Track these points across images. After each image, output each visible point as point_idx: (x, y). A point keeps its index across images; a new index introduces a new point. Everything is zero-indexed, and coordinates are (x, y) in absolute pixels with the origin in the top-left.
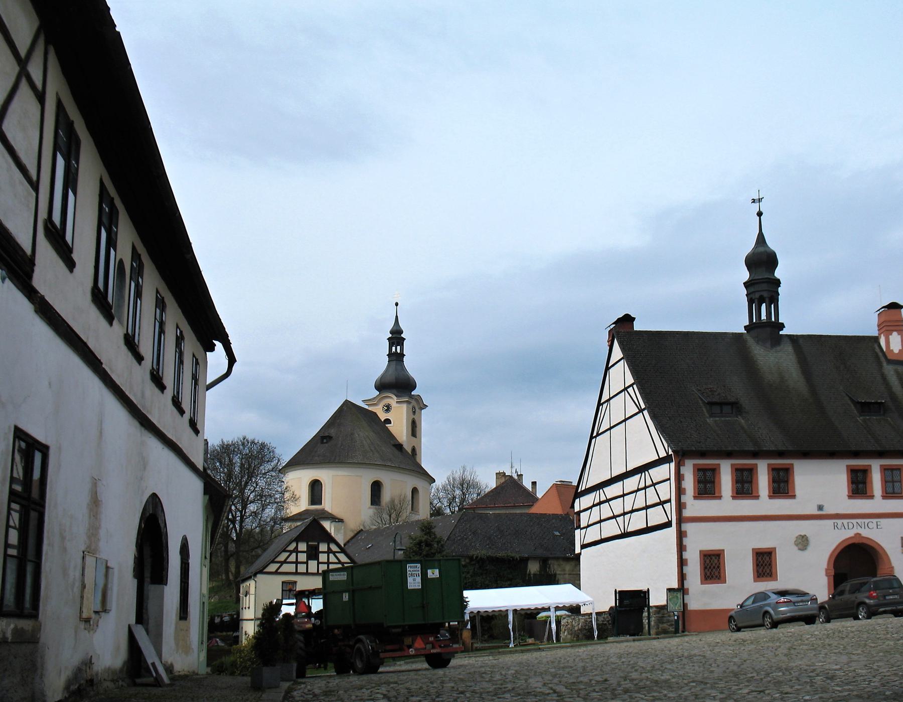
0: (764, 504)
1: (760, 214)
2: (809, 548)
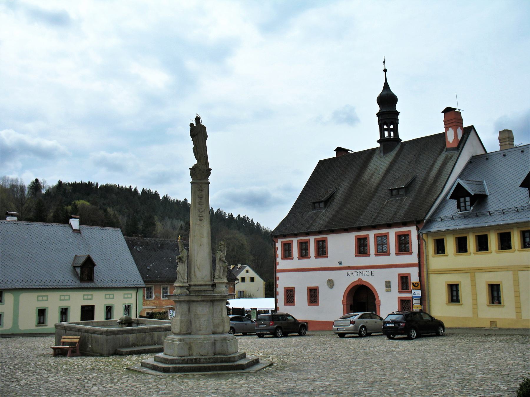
0: (313, 262)
2: (334, 287)
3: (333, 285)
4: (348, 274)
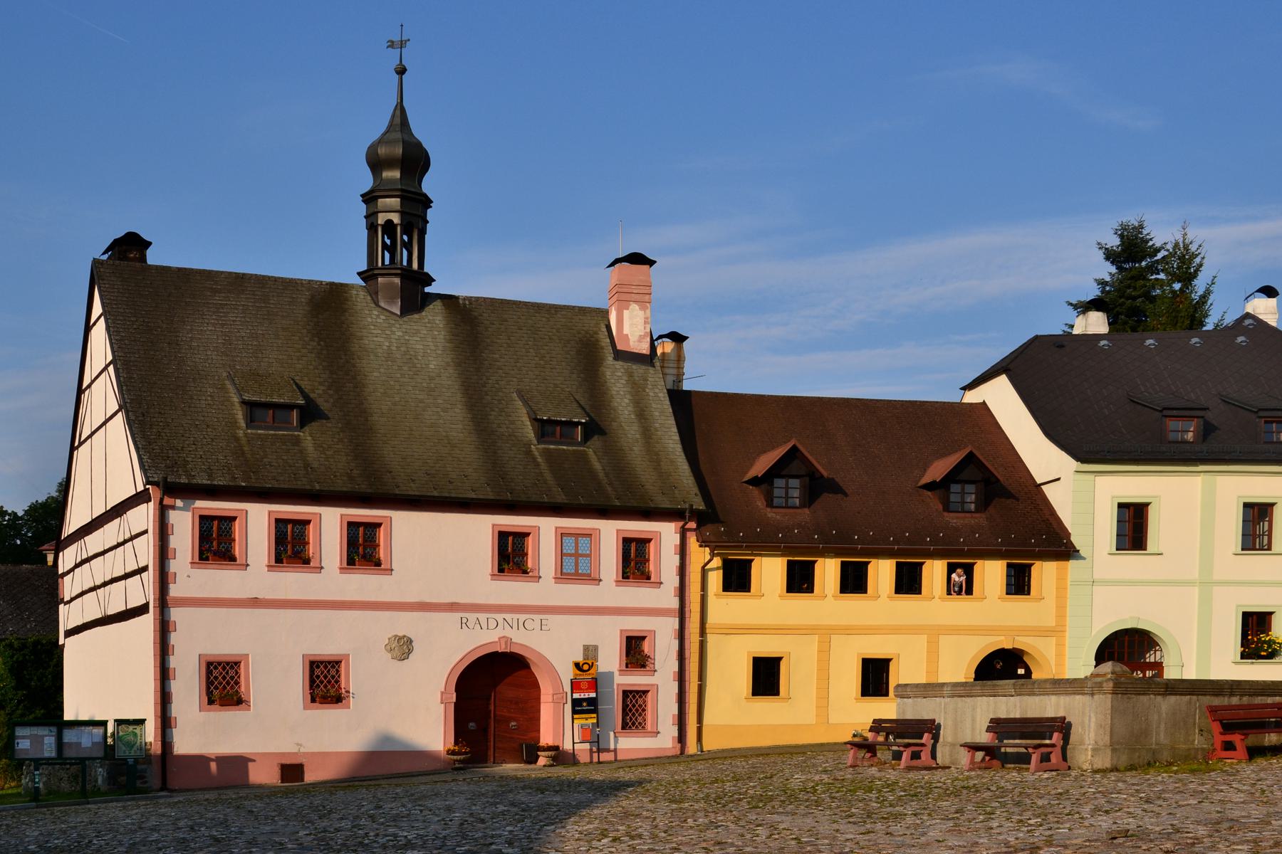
0: (330, 574)
1: (401, 71)
3: (410, 651)
4: (463, 623)
